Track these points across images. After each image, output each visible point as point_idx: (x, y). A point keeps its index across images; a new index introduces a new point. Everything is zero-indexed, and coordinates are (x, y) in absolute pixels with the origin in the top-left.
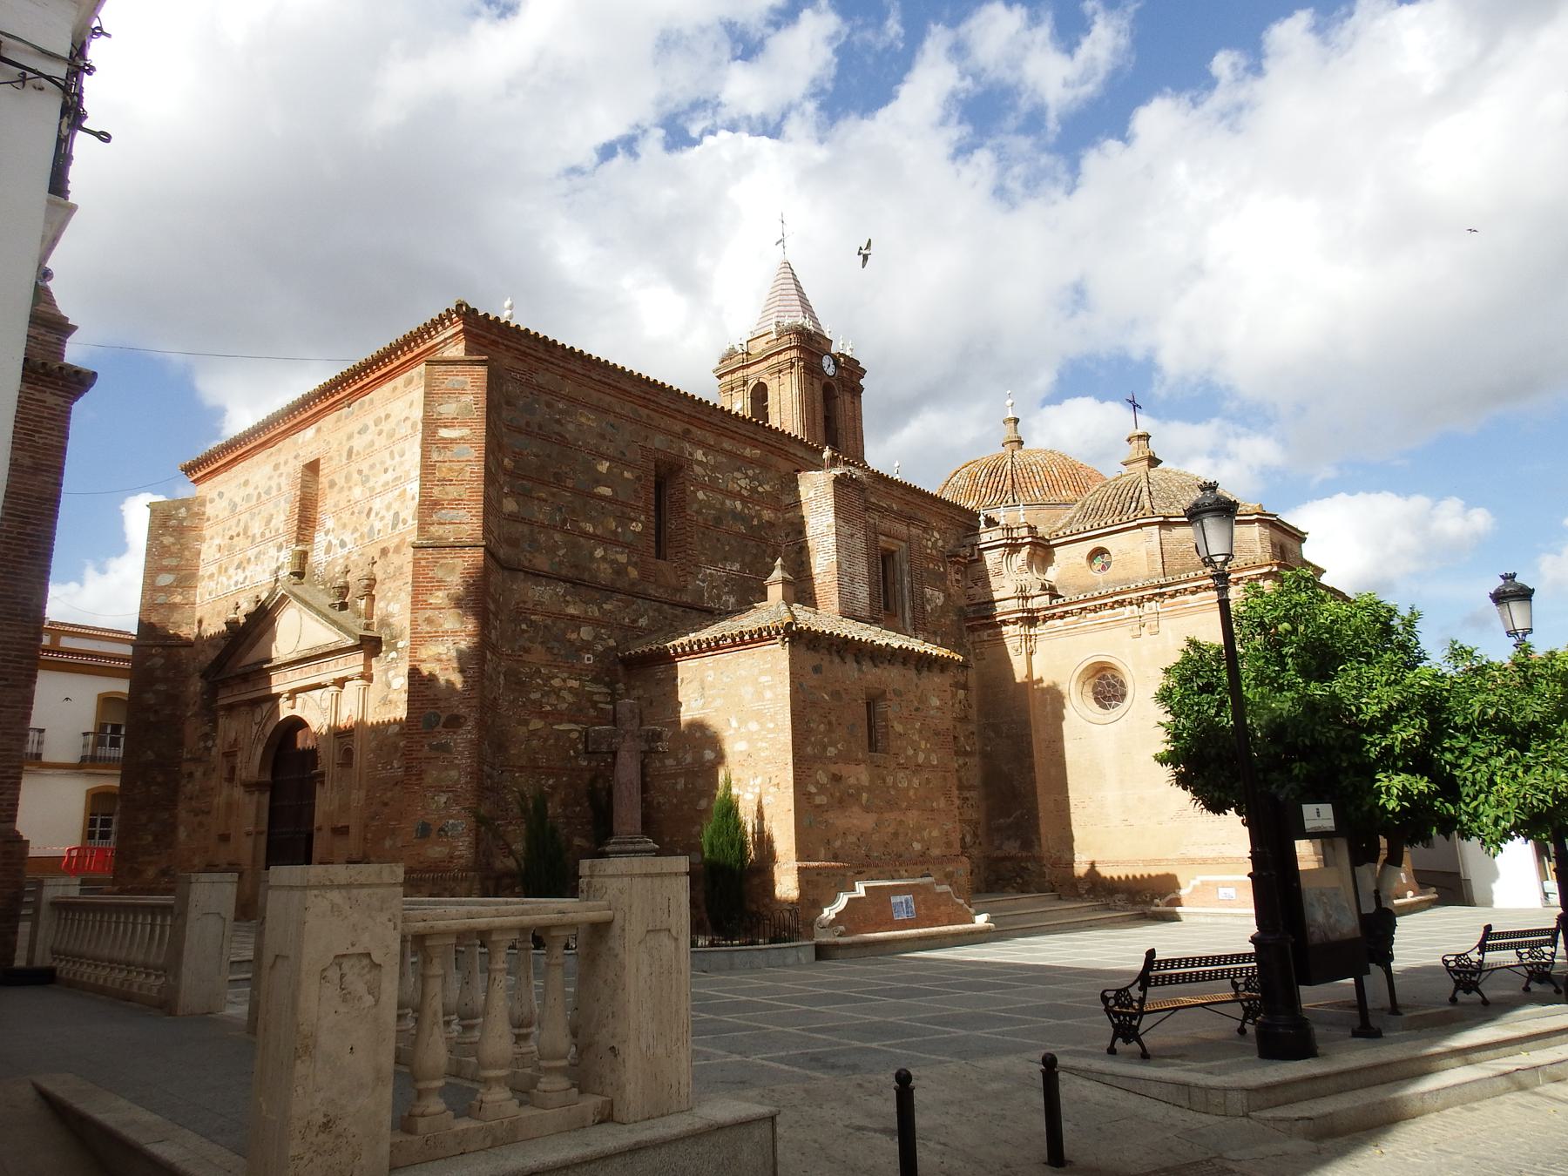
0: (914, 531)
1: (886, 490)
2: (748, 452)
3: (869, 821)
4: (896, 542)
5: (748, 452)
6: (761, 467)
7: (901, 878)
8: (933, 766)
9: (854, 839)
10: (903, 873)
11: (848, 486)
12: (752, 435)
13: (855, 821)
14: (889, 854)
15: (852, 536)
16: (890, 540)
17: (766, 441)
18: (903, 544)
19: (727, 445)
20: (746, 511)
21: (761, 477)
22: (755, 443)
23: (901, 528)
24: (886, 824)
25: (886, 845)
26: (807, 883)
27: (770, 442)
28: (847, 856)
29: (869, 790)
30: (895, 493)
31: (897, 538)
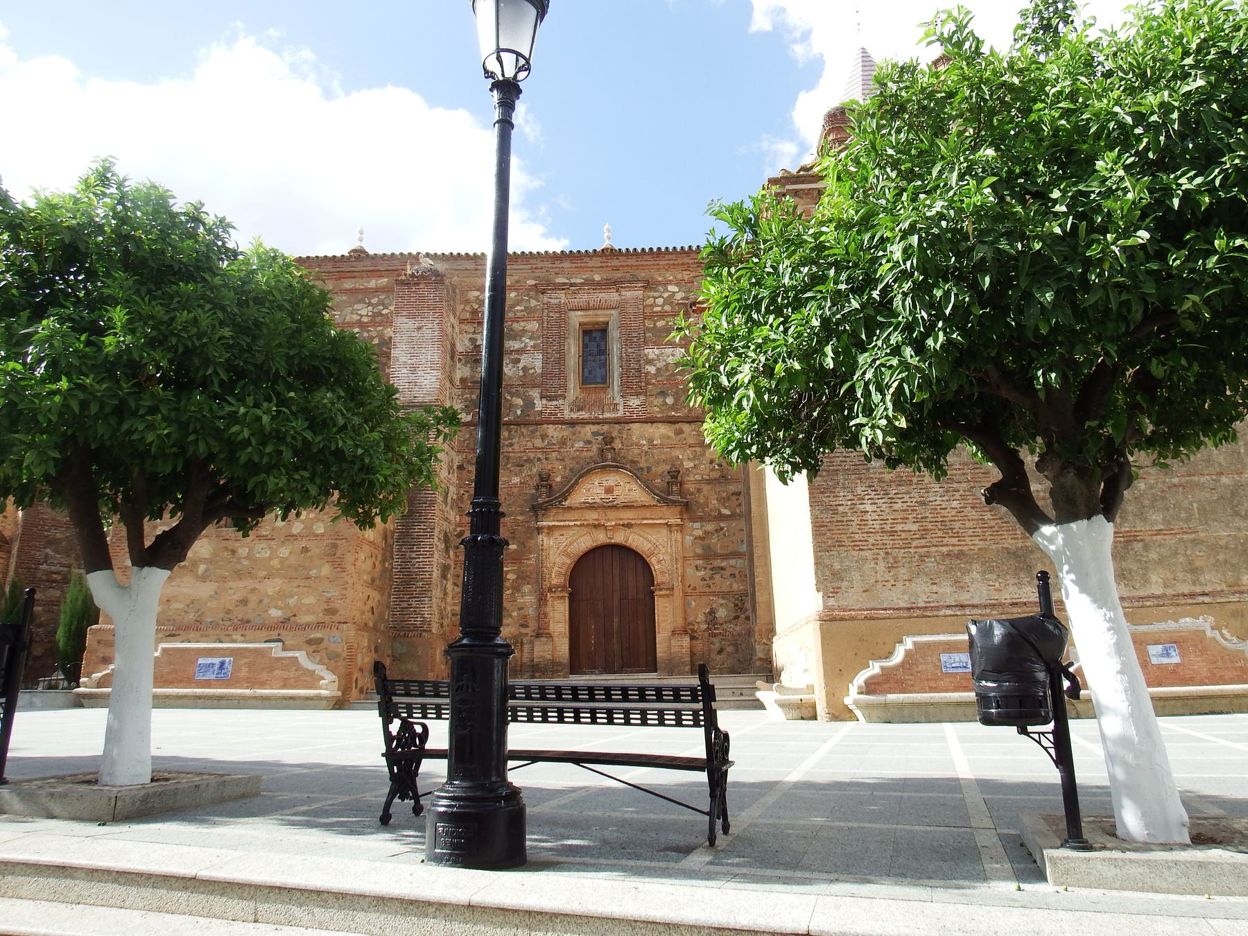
0: (628, 294)
1: (574, 265)
2: (372, 284)
3: (206, 589)
4: (599, 312)
5: (372, 284)
6: (384, 292)
7: (234, 641)
8: (317, 536)
9: (181, 606)
10: (239, 637)
11: (417, 284)
12: (372, 268)
13: (186, 590)
14: (230, 620)
15: (419, 328)
16: (591, 312)
17: (389, 268)
18: (613, 312)
19: (348, 284)
20: (366, 335)
21: (386, 301)
22: (378, 274)
23: (612, 296)
24: (230, 591)
25: (228, 612)
26: (99, 642)
27: (394, 268)
28: (169, 621)
29: (209, 561)
30: (589, 265)
31: (600, 308)
